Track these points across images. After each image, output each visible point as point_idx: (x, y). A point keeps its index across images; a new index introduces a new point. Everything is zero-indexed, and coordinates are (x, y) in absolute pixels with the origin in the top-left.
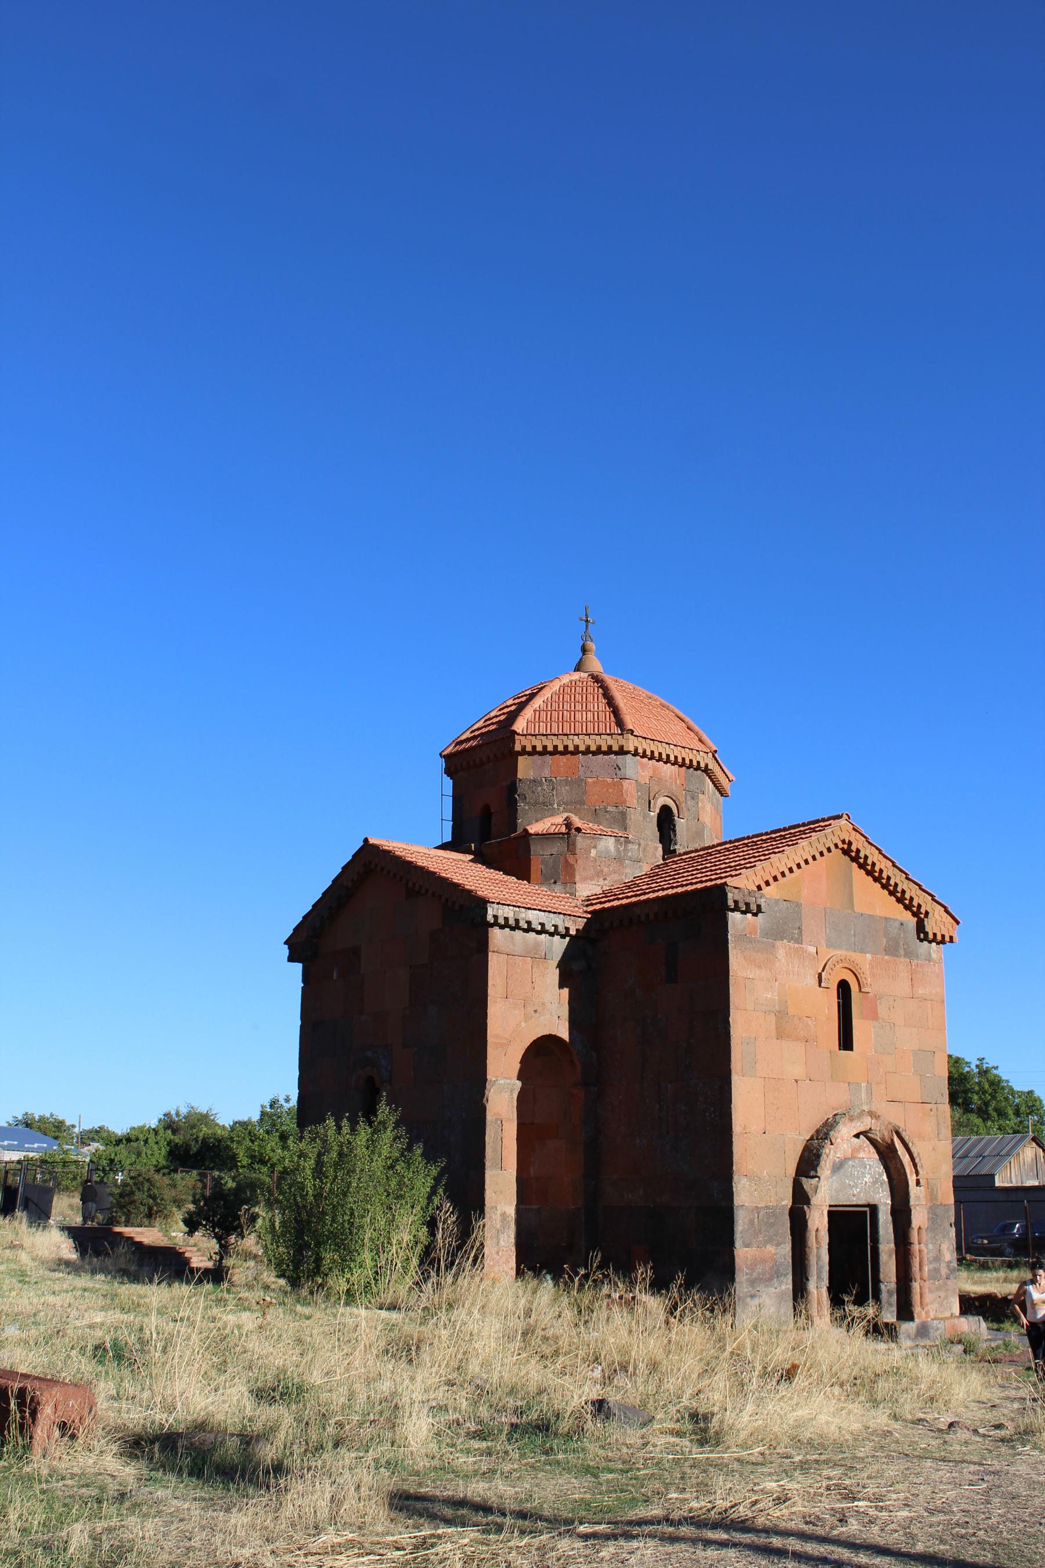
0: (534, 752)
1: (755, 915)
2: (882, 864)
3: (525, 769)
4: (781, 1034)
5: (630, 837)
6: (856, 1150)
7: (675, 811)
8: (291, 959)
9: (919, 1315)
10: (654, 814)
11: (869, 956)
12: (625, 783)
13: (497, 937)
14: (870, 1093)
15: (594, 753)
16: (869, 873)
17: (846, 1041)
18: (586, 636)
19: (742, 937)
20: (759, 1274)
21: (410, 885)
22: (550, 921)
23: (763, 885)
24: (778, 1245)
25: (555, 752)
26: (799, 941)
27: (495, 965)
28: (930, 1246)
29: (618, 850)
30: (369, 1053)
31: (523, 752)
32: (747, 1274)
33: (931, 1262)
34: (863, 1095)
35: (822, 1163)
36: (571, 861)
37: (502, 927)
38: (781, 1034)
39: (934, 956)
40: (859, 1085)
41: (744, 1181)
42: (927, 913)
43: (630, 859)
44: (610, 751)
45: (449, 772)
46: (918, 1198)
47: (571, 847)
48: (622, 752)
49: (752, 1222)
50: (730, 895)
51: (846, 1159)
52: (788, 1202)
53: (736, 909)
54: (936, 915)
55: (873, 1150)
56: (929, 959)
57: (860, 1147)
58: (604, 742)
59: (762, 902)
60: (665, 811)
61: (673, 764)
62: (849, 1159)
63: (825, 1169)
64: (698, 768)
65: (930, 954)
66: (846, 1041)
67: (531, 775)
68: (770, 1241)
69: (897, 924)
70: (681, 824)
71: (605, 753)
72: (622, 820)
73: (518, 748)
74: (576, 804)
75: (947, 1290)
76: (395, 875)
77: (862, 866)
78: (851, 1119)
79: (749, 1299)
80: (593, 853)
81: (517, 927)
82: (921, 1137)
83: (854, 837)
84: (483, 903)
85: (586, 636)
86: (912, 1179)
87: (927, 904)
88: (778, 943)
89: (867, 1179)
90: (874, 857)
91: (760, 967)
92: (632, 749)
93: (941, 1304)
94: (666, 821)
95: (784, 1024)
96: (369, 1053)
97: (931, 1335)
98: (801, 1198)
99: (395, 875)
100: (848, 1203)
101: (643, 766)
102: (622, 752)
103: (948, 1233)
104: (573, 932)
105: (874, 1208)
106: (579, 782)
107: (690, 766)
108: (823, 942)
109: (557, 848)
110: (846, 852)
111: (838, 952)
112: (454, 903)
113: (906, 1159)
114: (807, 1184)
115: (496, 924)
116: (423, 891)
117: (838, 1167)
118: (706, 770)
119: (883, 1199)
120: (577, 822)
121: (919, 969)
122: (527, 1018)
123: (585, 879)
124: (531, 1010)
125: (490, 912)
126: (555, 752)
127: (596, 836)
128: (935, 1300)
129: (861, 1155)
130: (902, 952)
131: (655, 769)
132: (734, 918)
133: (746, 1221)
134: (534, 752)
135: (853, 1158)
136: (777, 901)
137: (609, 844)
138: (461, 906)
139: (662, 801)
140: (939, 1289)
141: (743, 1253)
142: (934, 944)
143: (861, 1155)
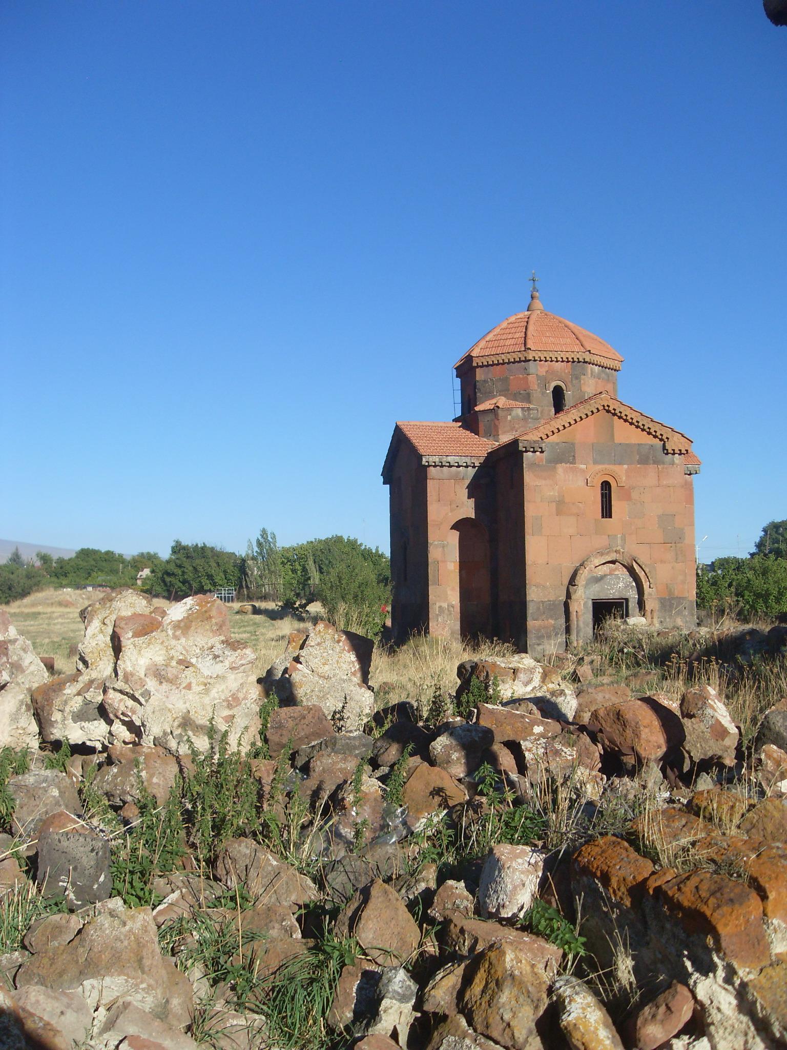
0: (482, 366)
1: (542, 452)
2: (631, 415)
3: (480, 375)
4: (559, 513)
5: (531, 406)
6: (612, 571)
7: (564, 388)
8: (384, 483)
10: (549, 392)
11: (625, 466)
12: (530, 377)
13: (432, 471)
14: (624, 539)
15: (513, 363)
16: (626, 421)
17: (607, 512)
19: (533, 465)
22: (462, 461)
23: (544, 437)
24: (556, 619)
25: (493, 365)
26: (573, 463)
27: (431, 486)
29: (524, 415)
31: (478, 367)
34: (619, 542)
35: (578, 578)
36: (497, 422)
37: (435, 466)
38: (559, 513)
39: (677, 461)
40: (616, 536)
41: (534, 588)
43: (532, 418)
44: (520, 362)
46: (650, 594)
47: (496, 415)
48: (527, 361)
49: (539, 608)
50: (520, 444)
51: (605, 575)
52: (563, 598)
53: (526, 451)
54: (675, 439)
55: (625, 570)
56: (673, 463)
57: (616, 569)
58: (517, 356)
59: (543, 445)
61: (563, 361)
63: (581, 580)
64: (579, 362)
66: (607, 512)
67: (483, 378)
68: (551, 617)
70: (568, 394)
71: (518, 362)
72: (527, 398)
73: (475, 364)
74: (505, 392)
77: (620, 418)
78: (602, 554)
80: (509, 418)
81: (442, 466)
82: (662, 562)
83: (611, 403)
84: (420, 457)
86: (646, 585)
87: (666, 433)
88: (559, 466)
89: (621, 585)
90: (626, 411)
91: (545, 479)
92: (531, 358)
94: (558, 394)
95: (561, 506)
98: (569, 596)
101: (541, 366)
102: (527, 361)
104: (477, 464)
105: (627, 600)
106: (506, 380)
107: (574, 362)
108: (591, 462)
109: (490, 417)
110: (608, 411)
111: (600, 467)
113: (642, 575)
114: (572, 589)
115: (429, 466)
117: (599, 579)
118: (585, 362)
119: (633, 595)
120: (502, 401)
122: (452, 511)
123: (504, 433)
124: (454, 506)
125: (424, 460)
126: (493, 365)
127: (509, 410)
131: (549, 366)
132: (528, 456)
134: (482, 366)
135: (611, 574)
136: (557, 444)
137: (519, 412)
141: (531, 624)
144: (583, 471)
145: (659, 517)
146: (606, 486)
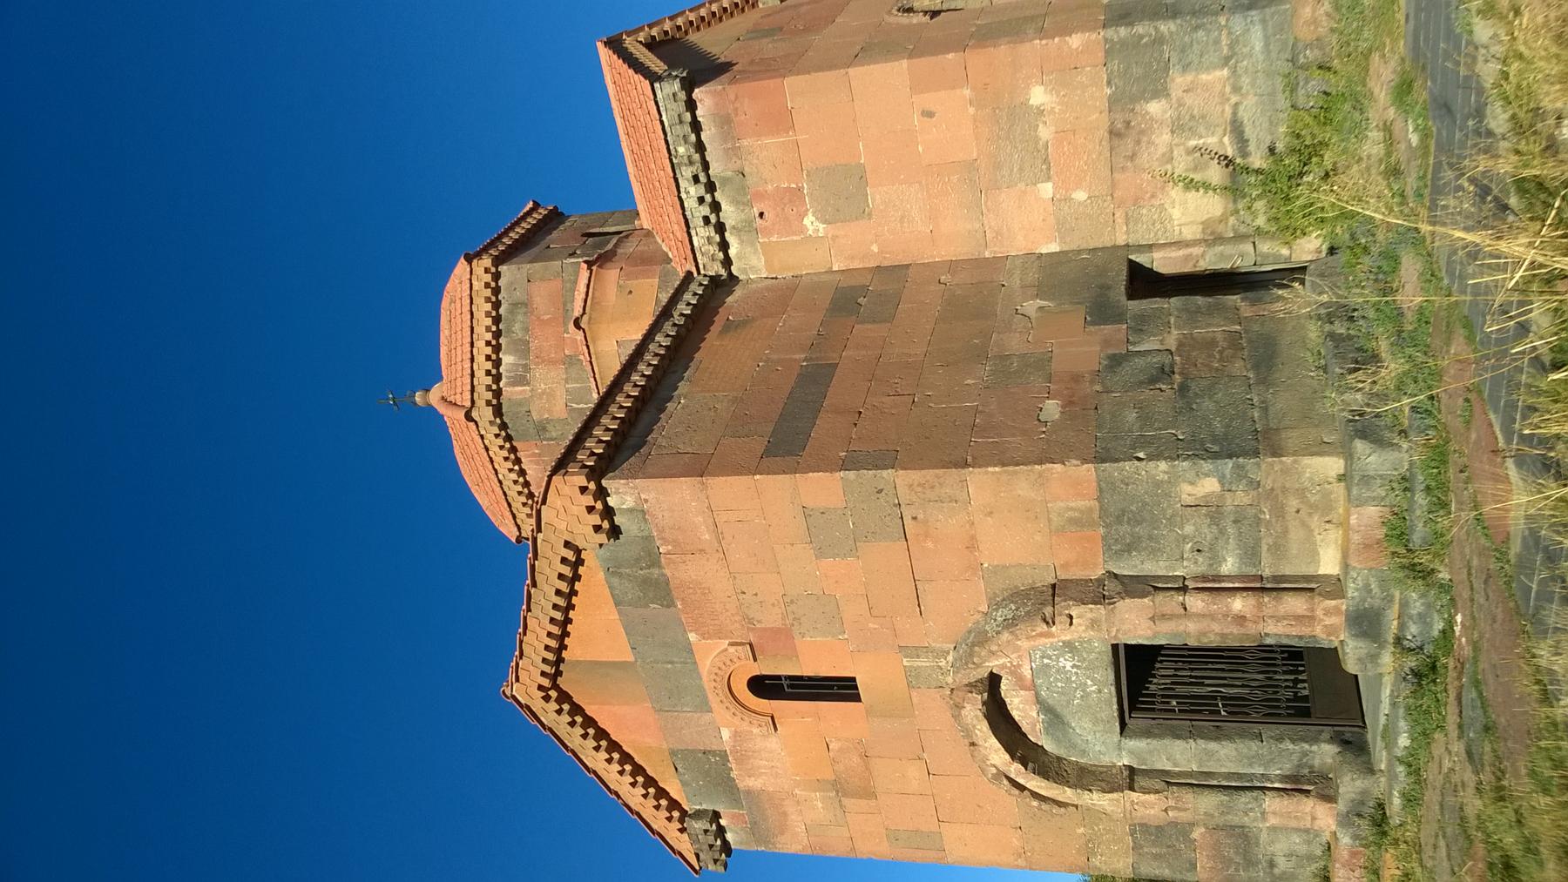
6: (1020, 683)
9: (1331, 630)
11: (692, 637)
20: (1236, 853)
28: (1189, 529)
32: (1237, 870)
33: (1222, 532)
34: (923, 662)
38: (868, 793)
39: (629, 502)
49: (1156, 857)
51: (1039, 700)
56: (639, 512)
62: (1037, 695)
65: (631, 510)
69: (615, 581)
75: (1284, 490)
79: (1276, 871)
82: (972, 545)
88: (741, 785)
91: (785, 814)
93: (1314, 508)
97: (1377, 603)
100: (1115, 700)
103: (1158, 484)
121: (667, 535)
128: (1304, 524)
129: (1027, 673)
130: (656, 571)
133: (1155, 864)
135: (1033, 687)
136: (684, 784)
140: (1279, 512)
142: (611, 501)
143: (1027, 673)
144: (736, 735)
145: (820, 554)
146: (764, 686)
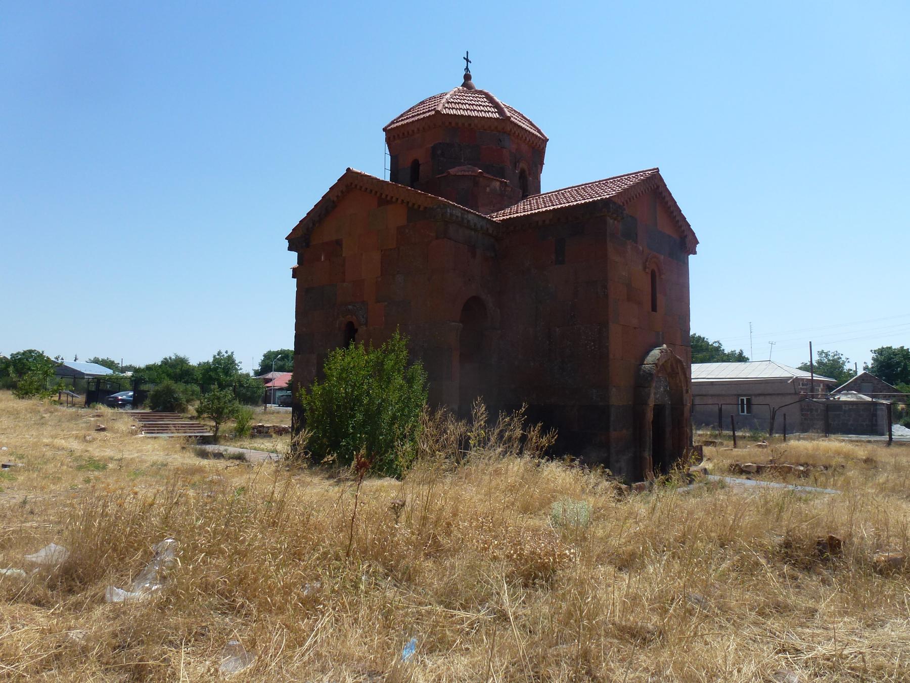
8: (290, 249)
18: (467, 69)
21: (384, 196)
30: (350, 307)
41: (614, 389)
42: (686, 236)
45: (389, 141)
60: (522, 172)
76: (371, 191)
80: (488, 189)
85: (467, 69)
96: (350, 307)
99: (371, 191)
112: (419, 206)
116: (394, 199)
138: (426, 208)
139: (522, 165)
